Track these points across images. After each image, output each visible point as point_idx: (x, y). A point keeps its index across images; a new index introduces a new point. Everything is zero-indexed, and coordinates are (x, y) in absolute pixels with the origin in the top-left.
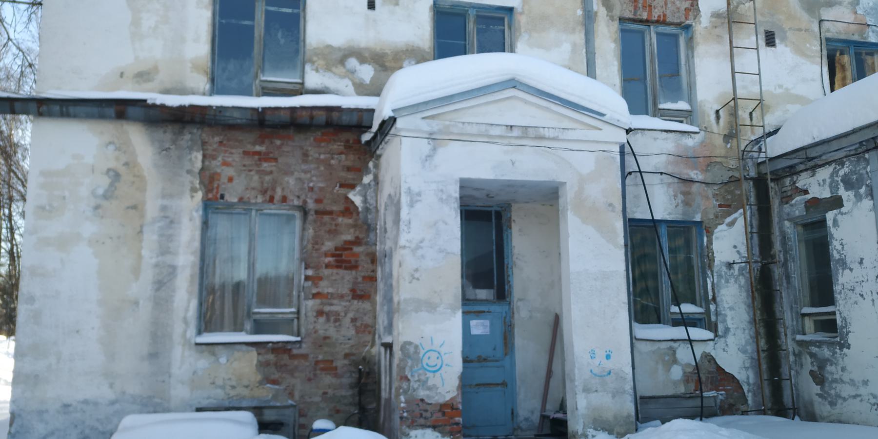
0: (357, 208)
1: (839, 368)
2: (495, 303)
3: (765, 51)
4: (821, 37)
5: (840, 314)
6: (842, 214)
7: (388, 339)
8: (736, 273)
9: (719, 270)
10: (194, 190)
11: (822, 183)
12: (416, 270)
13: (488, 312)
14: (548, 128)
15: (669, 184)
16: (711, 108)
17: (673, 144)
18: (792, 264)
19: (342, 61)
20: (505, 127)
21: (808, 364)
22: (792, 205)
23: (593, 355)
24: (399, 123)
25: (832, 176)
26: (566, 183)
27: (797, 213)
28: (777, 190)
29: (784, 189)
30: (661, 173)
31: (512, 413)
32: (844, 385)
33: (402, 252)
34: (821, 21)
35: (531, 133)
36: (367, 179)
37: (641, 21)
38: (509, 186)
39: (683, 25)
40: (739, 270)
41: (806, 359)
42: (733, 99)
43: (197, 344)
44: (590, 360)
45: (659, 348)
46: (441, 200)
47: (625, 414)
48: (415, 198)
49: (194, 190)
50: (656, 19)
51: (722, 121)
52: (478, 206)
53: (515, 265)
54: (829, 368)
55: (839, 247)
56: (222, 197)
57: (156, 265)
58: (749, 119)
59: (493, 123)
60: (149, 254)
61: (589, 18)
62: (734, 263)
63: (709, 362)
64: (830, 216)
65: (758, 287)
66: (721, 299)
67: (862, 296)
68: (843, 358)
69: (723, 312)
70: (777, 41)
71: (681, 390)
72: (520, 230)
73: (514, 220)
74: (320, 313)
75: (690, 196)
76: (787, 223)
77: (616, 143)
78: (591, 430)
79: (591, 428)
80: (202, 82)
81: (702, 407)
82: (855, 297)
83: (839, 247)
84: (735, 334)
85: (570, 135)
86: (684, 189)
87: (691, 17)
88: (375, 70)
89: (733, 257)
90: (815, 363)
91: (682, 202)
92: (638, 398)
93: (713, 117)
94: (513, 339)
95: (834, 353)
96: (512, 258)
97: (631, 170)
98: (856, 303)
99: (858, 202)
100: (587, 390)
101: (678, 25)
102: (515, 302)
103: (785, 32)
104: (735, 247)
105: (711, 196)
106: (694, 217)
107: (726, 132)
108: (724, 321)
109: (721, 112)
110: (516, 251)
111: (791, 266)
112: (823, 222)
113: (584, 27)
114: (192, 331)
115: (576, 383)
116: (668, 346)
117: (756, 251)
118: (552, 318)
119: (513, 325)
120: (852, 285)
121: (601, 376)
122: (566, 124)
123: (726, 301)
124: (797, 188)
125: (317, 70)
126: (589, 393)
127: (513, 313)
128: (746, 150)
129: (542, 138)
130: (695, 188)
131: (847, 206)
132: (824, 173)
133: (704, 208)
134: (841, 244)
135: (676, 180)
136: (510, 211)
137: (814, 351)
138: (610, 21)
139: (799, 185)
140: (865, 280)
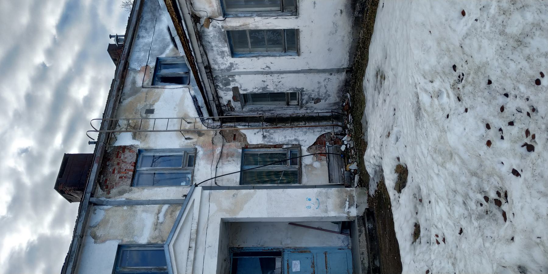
1: (313, 92)
2: (283, 257)
3: (156, 115)
4: (151, 88)
5: (288, 91)
6: (241, 87)
8: (268, 134)
9: (266, 142)
11: (226, 94)
13: (288, 261)
14: (192, 227)
15: (223, 164)
16: (184, 142)
17: (202, 161)
18: (264, 108)
20: (190, 251)
21: (311, 104)
22: (235, 107)
23: (309, 207)
25: (223, 90)
26: (222, 219)
27: (240, 105)
28: (227, 113)
29: (227, 110)
30: (217, 167)
31: (340, 249)
32: (320, 91)
35: (194, 236)
38: (221, 249)
39: (138, 154)
40: (266, 133)
41: (308, 105)
42: (180, 131)
44: (312, 209)
45: (305, 172)
47: (337, 193)
50: (133, 167)
51: (191, 137)
52: (230, 266)
53: (263, 245)
54: (313, 96)
55: (257, 89)
58: (191, 124)
59: (187, 257)
61: (130, 203)
62: (263, 135)
63: (311, 149)
64: (241, 92)
65: (275, 124)
66: (280, 141)
67: (279, 82)
68: (308, 91)
69: (287, 141)
70: (151, 108)
71: (325, 163)
72: (244, 242)
73: (239, 246)
75: (229, 154)
76: (244, 110)
77: (202, 192)
78: (345, 210)
79: (344, 210)
81: (333, 154)
82: (280, 85)
83: (257, 89)
84: (298, 136)
86: (225, 157)
90: (311, 102)
91: (231, 157)
92: (330, 184)
93: (189, 141)
94: (302, 248)
95: (306, 94)
96: (259, 247)
97: (214, 182)
98: (283, 84)
99: (236, 81)
100: (326, 211)
101: (138, 155)
102: (283, 246)
104: (255, 134)
105: (229, 144)
106: (240, 152)
107: (197, 135)
108: (291, 141)
110: (255, 245)
111: (264, 109)
112: (244, 95)
113: (133, 205)
115: (323, 216)
116: (304, 168)
117: (257, 124)
118: (291, 226)
119: (295, 248)
120: (274, 86)
121: (319, 204)
123: (282, 139)
124: (227, 104)
126: (328, 210)
127: (288, 247)
128: (207, 126)
130: (225, 151)
131: (237, 85)
132: (221, 93)
133: (235, 148)
134: (255, 88)
135: (221, 160)
136: (233, 248)
137: (305, 102)
138: (132, 191)
139: (225, 103)
140: (272, 80)
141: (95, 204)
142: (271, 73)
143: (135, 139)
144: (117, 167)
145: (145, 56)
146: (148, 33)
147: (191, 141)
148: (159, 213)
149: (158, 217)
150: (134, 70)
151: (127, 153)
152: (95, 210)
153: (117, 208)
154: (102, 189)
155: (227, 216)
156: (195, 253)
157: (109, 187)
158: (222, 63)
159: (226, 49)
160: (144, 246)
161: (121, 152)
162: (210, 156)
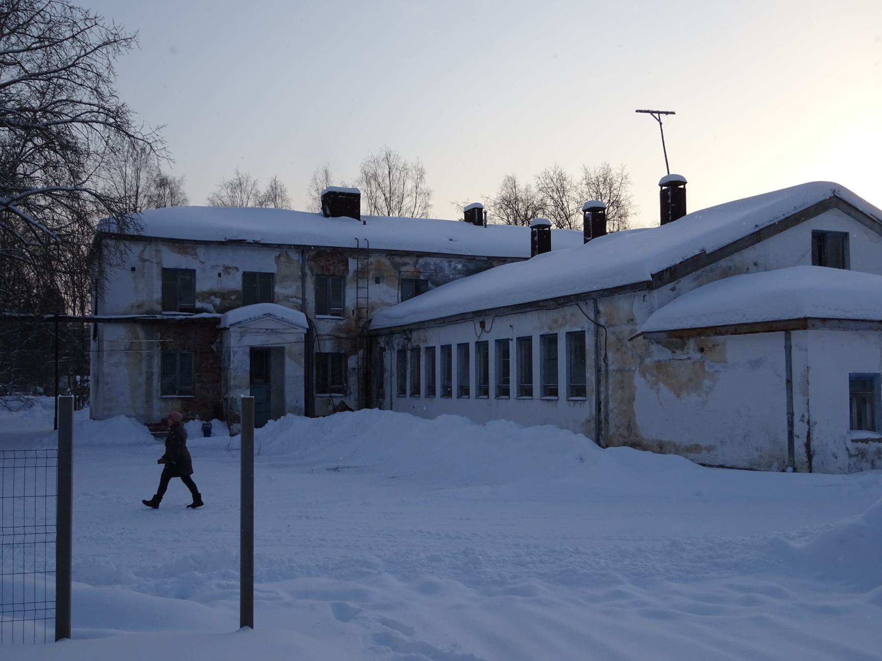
0: (214, 351)
7: (226, 396)
10: (158, 346)
12: (236, 376)
19: (209, 298)
24: (230, 330)
33: (231, 370)
36: (218, 341)
37: (325, 275)
43: (161, 398)
46: (244, 354)
49: (158, 346)
51: (355, 314)
56: (168, 348)
57: (147, 372)
60: (144, 369)
61: (303, 276)
64: (384, 353)
70: (380, 281)
74: (202, 388)
76: (377, 354)
80: (159, 308)
85: (288, 331)
87: (346, 272)
88: (221, 300)
93: (351, 312)
103: (383, 277)
108: (350, 389)
114: (159, 394)
122: (286, 327)
129: (278, 332)
132: (383, 339)
142: (391, 376)
143: (354, 272)
144: (331, 263)
145: (430, 269)
147: (351, 315)
148: (295, 297)
149: (293, 297)
150: (417, 263)
151: (342, 268)
152: (299, 252)
153: (300, 266)
154: (315, 254)
155: (287, 350)
156: (264, 333)
157: (317, 259)
158: (395, 343)
159: (400, 348)
160: (273, 288)
161: (344, 264)
162: (339, 329)
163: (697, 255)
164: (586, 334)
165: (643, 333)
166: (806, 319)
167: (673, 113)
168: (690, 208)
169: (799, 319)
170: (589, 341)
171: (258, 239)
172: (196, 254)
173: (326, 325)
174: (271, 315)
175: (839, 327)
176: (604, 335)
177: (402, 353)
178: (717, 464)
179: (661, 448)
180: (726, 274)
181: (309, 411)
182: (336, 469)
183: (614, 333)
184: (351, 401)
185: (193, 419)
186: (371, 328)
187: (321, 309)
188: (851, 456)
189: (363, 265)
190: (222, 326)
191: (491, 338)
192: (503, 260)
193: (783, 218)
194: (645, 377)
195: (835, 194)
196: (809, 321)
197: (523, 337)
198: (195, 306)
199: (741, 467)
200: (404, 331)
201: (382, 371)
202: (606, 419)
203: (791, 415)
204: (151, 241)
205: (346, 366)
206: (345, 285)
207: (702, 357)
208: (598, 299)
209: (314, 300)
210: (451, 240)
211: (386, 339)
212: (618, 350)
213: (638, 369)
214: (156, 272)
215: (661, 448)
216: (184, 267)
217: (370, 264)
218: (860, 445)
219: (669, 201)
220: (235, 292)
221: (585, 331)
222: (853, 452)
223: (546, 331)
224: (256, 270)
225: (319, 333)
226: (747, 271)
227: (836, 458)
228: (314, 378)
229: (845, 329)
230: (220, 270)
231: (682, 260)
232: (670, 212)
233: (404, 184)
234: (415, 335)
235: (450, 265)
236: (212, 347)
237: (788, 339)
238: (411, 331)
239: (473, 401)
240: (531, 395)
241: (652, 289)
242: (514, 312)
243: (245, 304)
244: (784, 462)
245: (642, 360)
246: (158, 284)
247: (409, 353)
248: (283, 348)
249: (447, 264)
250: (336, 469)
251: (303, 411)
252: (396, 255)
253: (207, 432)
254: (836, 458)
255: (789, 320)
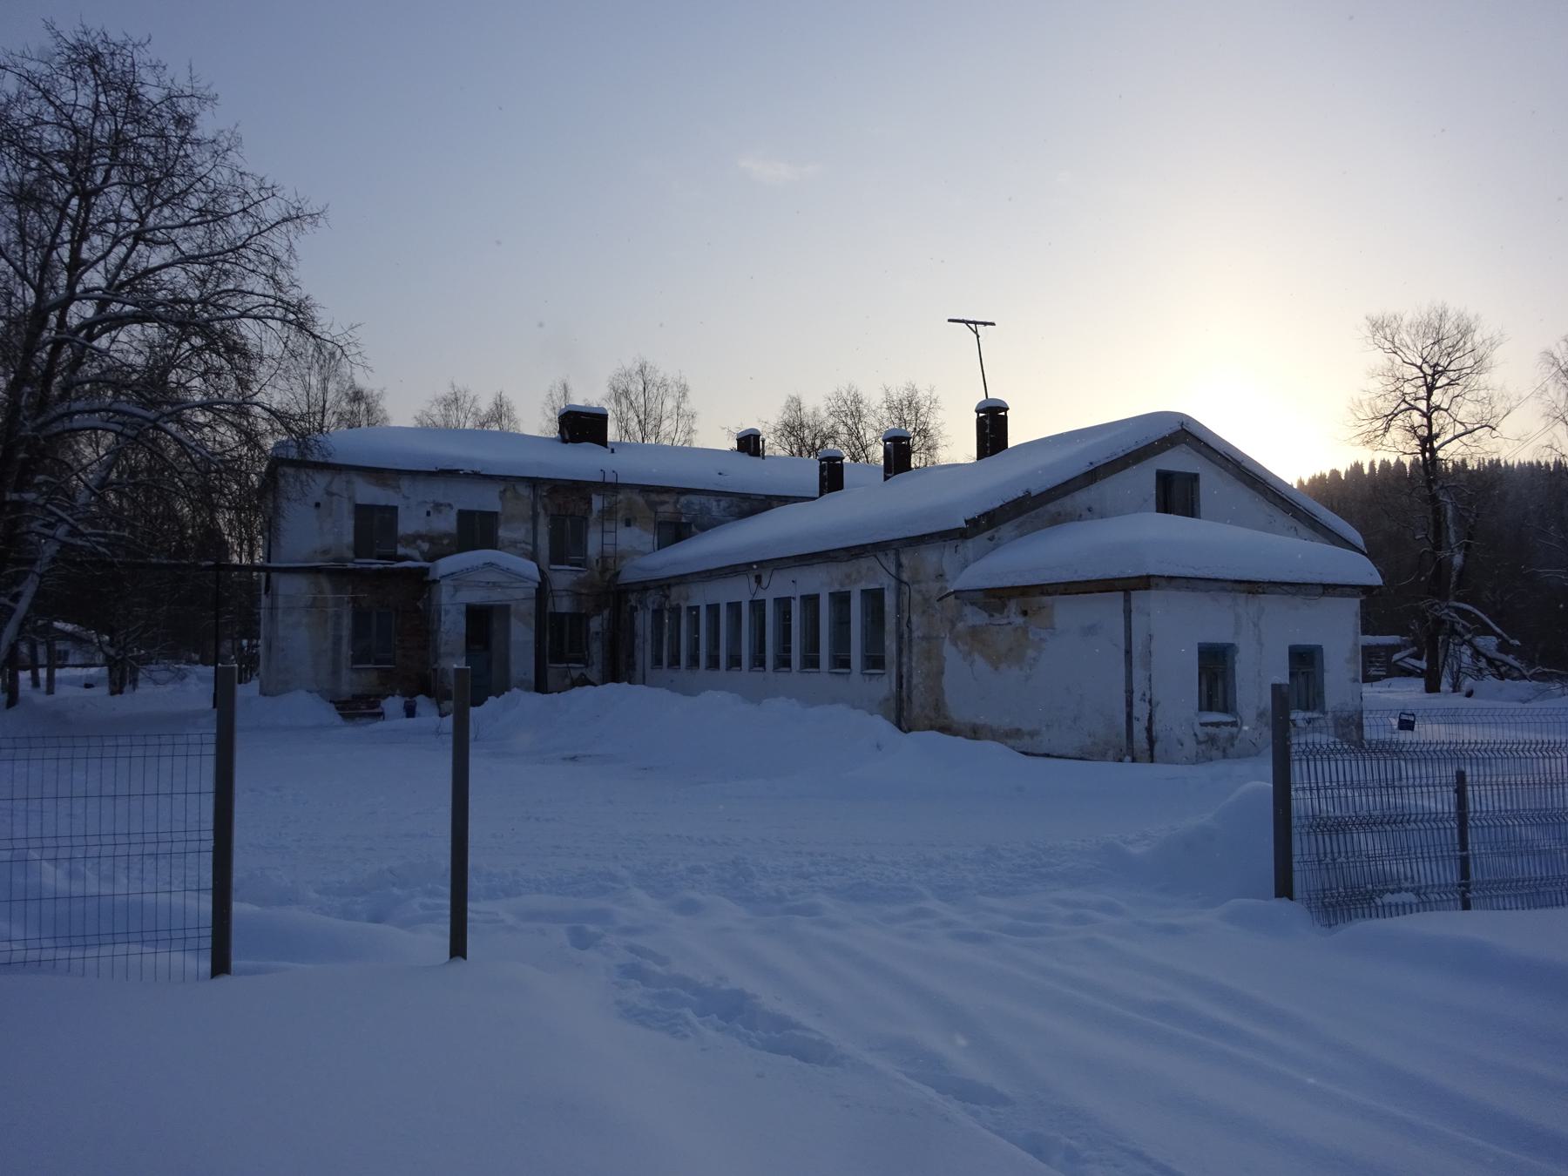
7: (435, 666)
24: (441, 583)
30: (567, 591)
34: (656, 513)
36: (425, 597)
37: (563, 516)
48: (447, 612)
70: (632, 523)
80: (350, 555)
85: (514, 585)
89: (600, 629)
93: (595, 564)
103: (636, 519)
109: (600, 561)
125: (403, 546)
141: (534, 486)
142: (644, 643)
145: (695, 510)
146: (724, 510)
148: (527, 543)
149: (520, 543)
150: (677, 502)
155: (512, 609)
159: (656, 607)
160: (497, 533)
163: (1019, 498)
164: (886, 592)
165: (954, 592)
166: (1149, 577)
167: (993, 324)
168: (1013, 440)
169: (1140, 577)
170: (890, 600)
171: (477, 469)
172: (399, 488)
173: (563, 577)
174: (493, 564)
175: (1187, 588)
176: (908, 594)
177: (658, 614)
178: (1042, 753)
179: (975, 732)
180: (1057, 520)
181: (541, 686)
182: (574, 759)
183: (920, 592)
184: (593, 674)
185: (393, 695)
186: (618, 583)
187: (557, 557)
188: (1199, 743)
189: (609, 503)
190: (430, 578)
191: (769, 596)
192: (785, 500)
193: (1121, 454)
194: (956, 645)
195: (1184, 427)
196: (1151, 580)
197: (808, 596)
198: (396, 552)
199: (1070, 755)
200: (661, 587)
201: (633, 635)
202: (909, 698)
203: (1130, 692)
204: (340, 470)
205: (588, 630)
206: (587, 527)
207: (1025, 622)
208: (901, 550)
209: (548, 546)
210: (720, 474)
211: (639, 596)
212: (924, 612)
213: (948, 635)
214: (347, 508)
215: (975, 732)
216: (383, 503)
217: (620, 502)
218: (1210, 729)
219: (988, 431)
220: (447, 535)
221: (883, 589)
222: (1202, 737)
223: (836, 588)
224: (475, 507)
225: (553, 588)
226: (1080, 518)
227: (1182, 745)
228: (547, 645)
229: (1194, 589)
230: (429, 507)
231: (1002, 503)
232: (988, 445)
233: (662, 403)
234: (674, 592)
235: (719, 505)
236: (418, 604)
237: (1127, 601)
238: (669, 586)
239: (745, 674)
240: (817, 666)
241: (967, 538)
242: (797, 564)
243: (461, 550)
244: (1121, 750)
245: (953, 625)
246: (348, 525)
247: (666, 615)
248: (507, 607)
249: (715, 504)
250: (574, 759)
251: (533, 685)
252: (652, 491)
253: (410, 712)
254: (1182, 745)
255: (1129, 578)
